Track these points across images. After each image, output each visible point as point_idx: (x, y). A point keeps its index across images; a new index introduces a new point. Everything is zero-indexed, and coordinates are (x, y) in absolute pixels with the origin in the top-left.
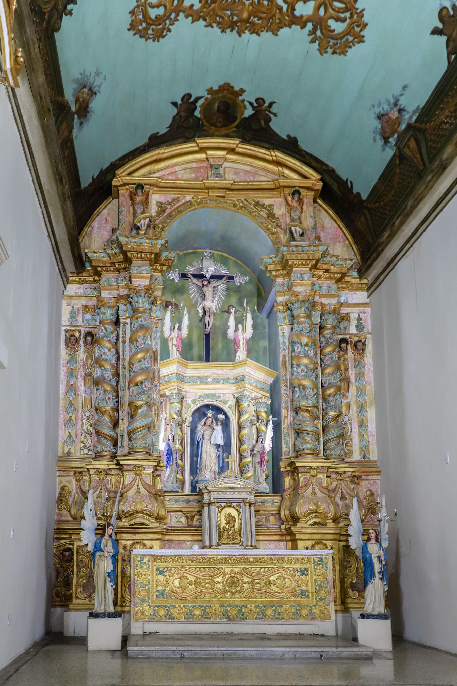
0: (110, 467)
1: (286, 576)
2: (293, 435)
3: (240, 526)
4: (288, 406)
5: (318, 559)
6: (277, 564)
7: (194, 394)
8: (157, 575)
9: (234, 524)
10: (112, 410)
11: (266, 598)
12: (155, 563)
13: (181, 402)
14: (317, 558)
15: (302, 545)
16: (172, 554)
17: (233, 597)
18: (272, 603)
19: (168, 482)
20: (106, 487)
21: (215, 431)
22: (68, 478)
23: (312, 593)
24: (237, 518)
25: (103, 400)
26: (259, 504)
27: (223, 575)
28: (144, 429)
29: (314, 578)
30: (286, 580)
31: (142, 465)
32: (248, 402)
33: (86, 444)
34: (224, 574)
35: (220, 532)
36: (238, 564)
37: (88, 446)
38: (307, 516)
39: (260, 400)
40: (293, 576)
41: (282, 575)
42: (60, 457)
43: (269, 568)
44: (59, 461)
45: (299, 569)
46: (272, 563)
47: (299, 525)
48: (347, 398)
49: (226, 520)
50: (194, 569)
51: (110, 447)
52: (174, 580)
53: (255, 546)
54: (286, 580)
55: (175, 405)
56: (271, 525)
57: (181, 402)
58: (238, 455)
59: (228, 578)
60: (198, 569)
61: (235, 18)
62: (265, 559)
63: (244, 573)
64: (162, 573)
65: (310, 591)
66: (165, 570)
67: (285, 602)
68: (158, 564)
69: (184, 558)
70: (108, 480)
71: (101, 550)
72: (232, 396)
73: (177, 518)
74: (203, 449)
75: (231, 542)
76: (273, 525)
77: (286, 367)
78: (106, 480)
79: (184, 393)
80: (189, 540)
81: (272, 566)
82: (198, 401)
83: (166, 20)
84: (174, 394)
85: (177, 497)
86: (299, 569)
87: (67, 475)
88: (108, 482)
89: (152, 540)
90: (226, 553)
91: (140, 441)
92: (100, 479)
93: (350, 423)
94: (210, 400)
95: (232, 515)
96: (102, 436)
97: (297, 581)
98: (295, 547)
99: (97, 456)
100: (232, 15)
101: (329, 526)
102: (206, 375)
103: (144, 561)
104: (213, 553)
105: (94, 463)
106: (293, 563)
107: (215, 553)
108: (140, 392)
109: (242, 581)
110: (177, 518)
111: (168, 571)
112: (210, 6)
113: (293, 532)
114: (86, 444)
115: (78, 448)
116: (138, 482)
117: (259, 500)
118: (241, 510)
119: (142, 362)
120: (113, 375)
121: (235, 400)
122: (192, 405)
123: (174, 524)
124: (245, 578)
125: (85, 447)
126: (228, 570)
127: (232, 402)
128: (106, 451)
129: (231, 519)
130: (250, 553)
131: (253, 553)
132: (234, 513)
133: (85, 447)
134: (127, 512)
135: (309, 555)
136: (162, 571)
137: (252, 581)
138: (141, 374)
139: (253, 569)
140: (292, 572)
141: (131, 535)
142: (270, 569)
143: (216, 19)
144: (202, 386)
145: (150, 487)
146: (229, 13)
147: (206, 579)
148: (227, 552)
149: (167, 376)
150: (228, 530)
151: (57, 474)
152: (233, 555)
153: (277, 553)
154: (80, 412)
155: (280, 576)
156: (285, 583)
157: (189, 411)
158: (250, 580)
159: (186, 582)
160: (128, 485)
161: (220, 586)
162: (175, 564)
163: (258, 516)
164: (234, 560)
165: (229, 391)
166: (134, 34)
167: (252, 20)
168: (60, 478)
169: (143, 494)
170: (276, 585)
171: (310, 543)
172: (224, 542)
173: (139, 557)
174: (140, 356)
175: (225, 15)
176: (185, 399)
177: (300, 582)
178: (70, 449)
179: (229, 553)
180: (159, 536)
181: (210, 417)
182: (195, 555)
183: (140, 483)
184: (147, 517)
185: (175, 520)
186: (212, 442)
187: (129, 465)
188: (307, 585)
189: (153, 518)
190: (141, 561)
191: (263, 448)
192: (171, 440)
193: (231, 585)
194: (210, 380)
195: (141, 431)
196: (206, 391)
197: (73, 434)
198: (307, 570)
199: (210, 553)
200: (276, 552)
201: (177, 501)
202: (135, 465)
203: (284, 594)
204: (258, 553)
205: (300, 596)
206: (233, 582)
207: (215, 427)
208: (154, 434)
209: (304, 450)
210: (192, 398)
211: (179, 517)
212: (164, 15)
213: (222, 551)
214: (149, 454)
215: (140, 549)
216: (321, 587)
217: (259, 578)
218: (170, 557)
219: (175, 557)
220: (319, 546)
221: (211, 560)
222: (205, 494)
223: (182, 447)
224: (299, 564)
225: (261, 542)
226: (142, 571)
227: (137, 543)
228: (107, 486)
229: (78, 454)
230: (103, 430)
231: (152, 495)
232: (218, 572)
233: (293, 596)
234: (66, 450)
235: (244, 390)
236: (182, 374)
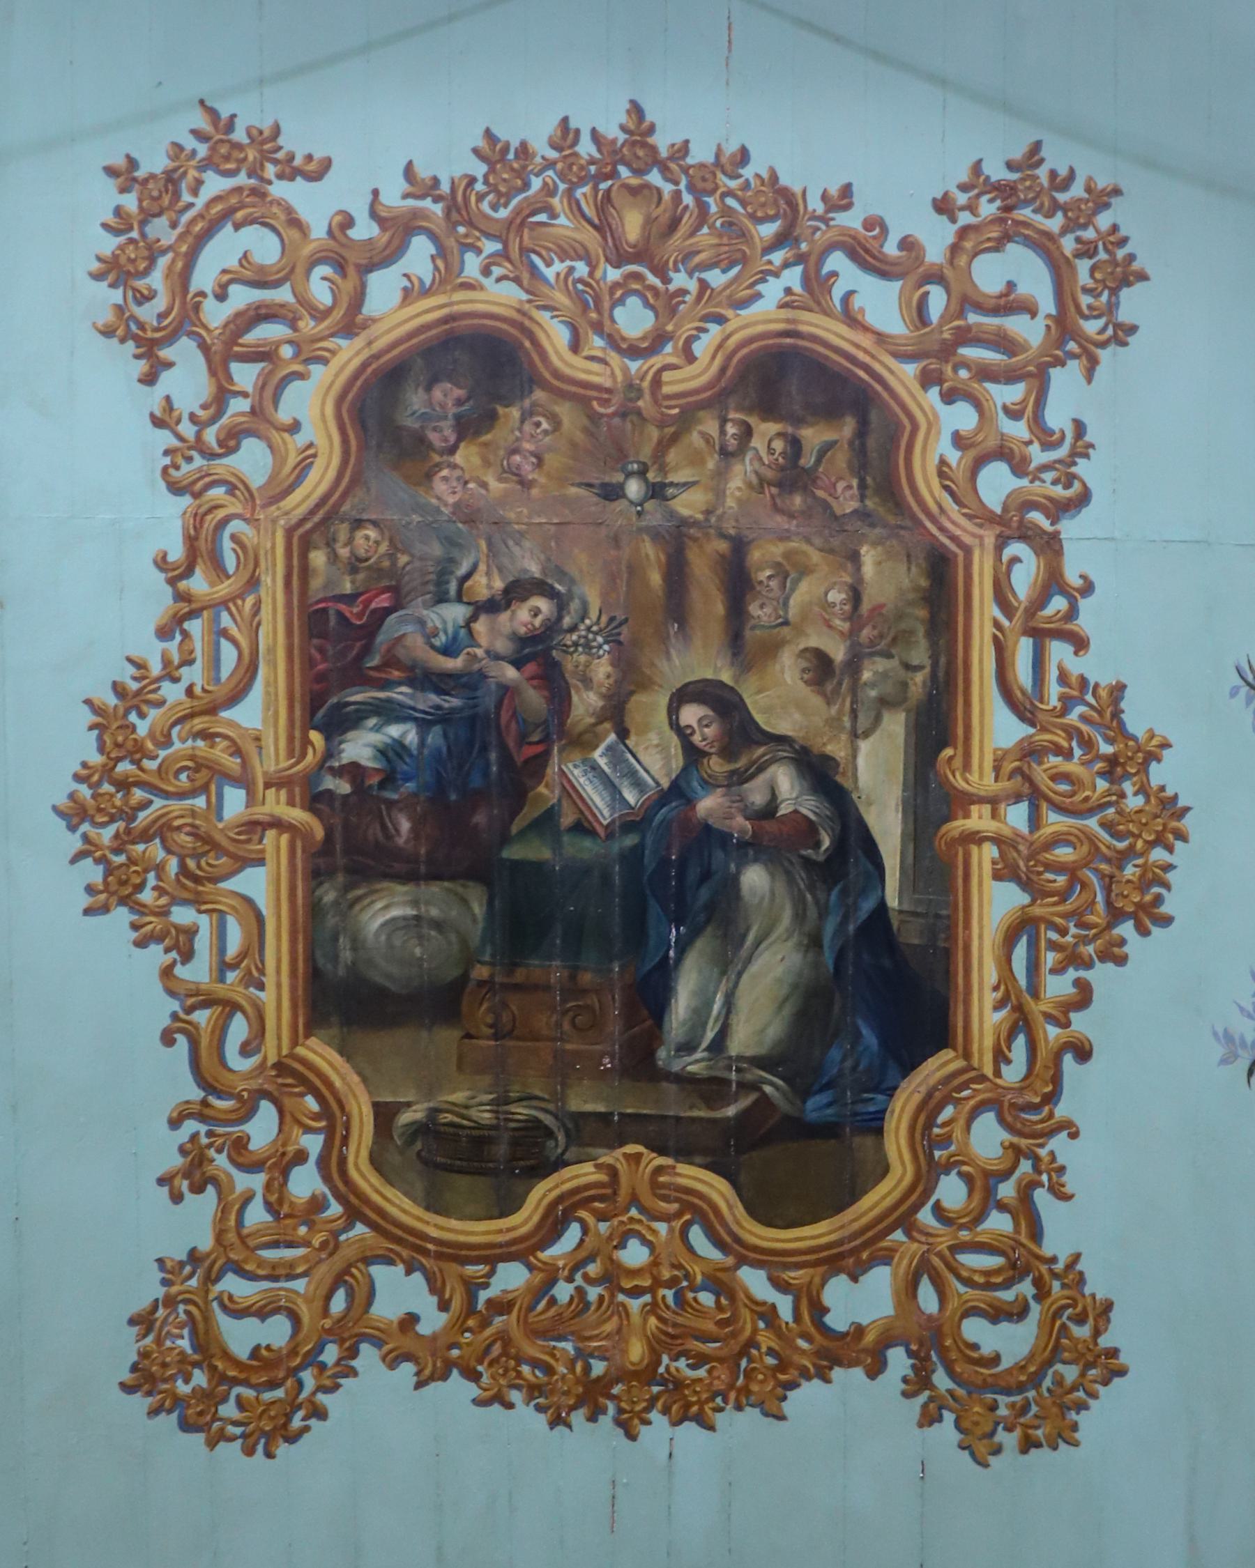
61: (598, 1368)
83: (301, 1367)
100: (583, 1355)
112: (485, 1323)
143: (519, 1375)
146: (568, 1346)
166: (154, 1412)
167: (667, 1368)
175: (553, 1356)
212: (293, 1352)
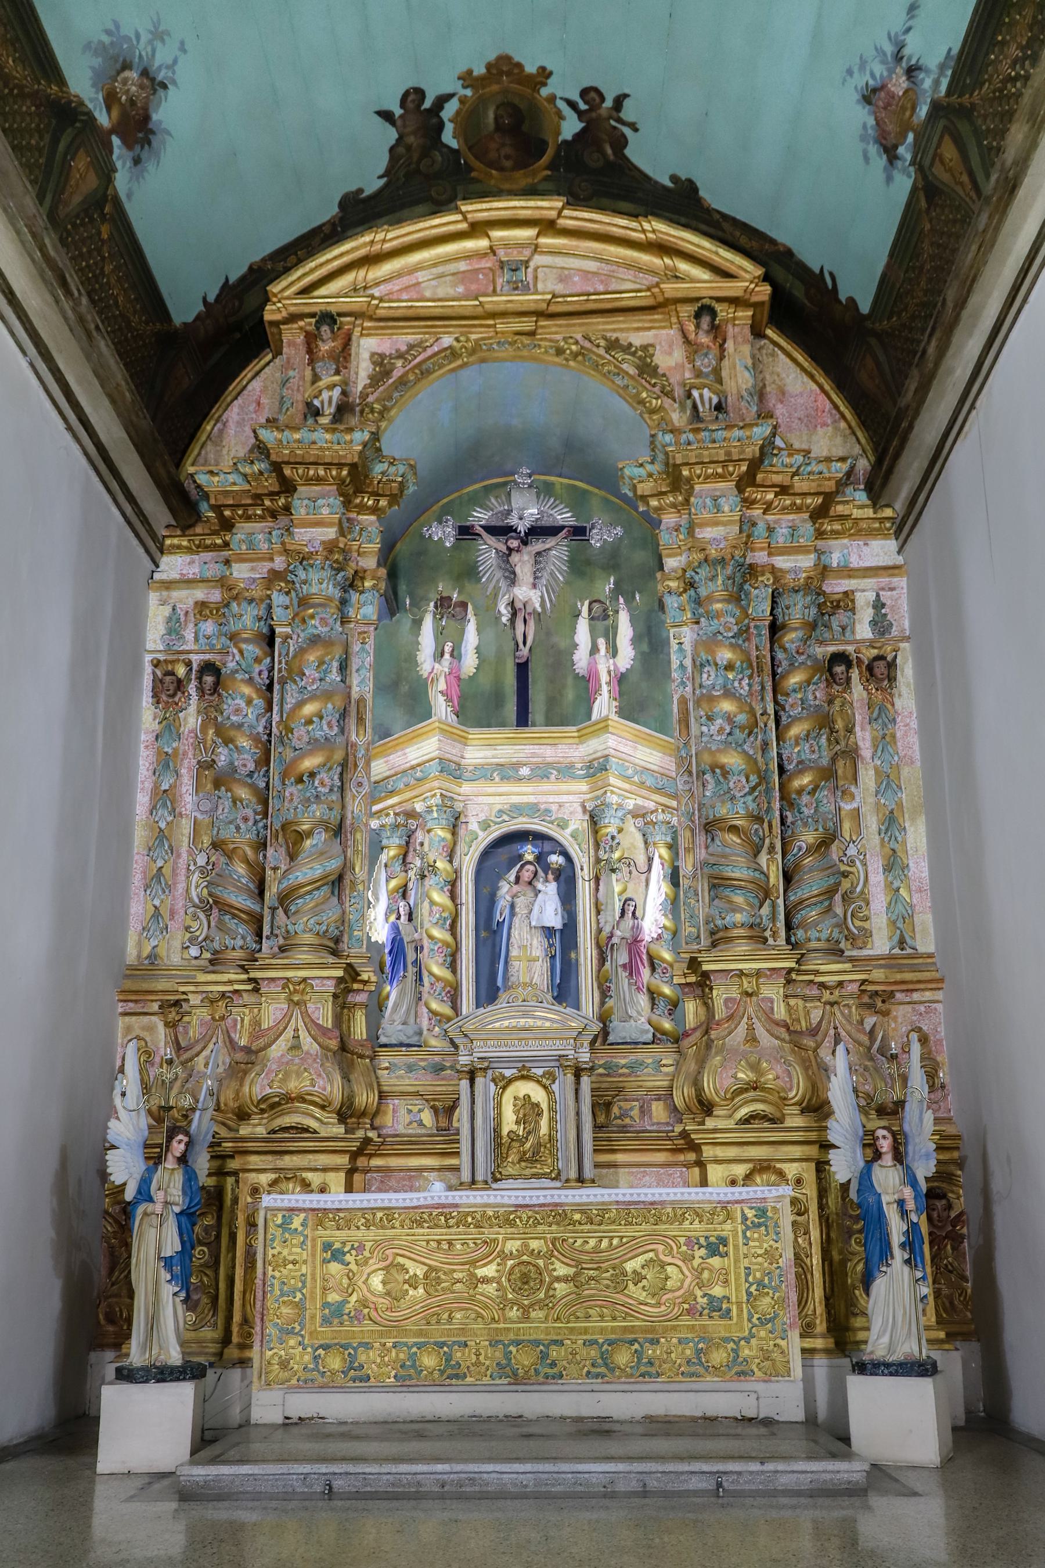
0: (237, 987)
1: (669, 1260)
2: (706, 894)
3: (550, 1128)
4: (693, 822)
5: (753, 1212)
6: (643, 1227)
7: (486, 808)
8: (325, 1261)
9: (537, 1122)
10: (251, 847)
11: (614, 1319)
12: (321, 1232)
13: (454, 830)
14: (751, 1208)
15: (720, 1175)
16: (365, 1205)
17: (526, 1317)
18: (632, 1333)
19: (394, 1021)
20: (229, 1036)
21: (540, 895)
22: (146, 1019)
23: (739, 1304)
24: (544, 1106)
25: (231, 822)
26: (621, 1071)
27: (498, 1260)
28: (318, 889)
29: (746, 1263)
30: (669, 1269)
31: (305, 980)
32: (617, 821)
33: (197, 933)
34: (504, 1256)
35: (499, 1145)
36: (540, 1228)
37: (200, 939)
38: (733, 1099)
39: (653, 817)
40: (688, 1259)
41: (657, 1255)
42: (131, 968)
43: (622, 1237)
44: (127, 977)
45: (702, 1241)
46: (631, 1224)
47: (710, 1123)
49: (516, 1112)
50: (424, 1243)
51: (243, 938)
52: (369, 1275)
53: (593, 1181)
54: (669, 1269)
55: (436, 835)
56: (653, 1125)
57: (454, 830)
58: (595, 952)
59: (513, 1268)
60: (433, 1244)
62: (613, 1214)
63: (556, 1253)
64: (337, 1256)
65: (734, 1300)
66: (346, 1250)
67: (666, 1330)
68: (328, 1232)
69: (396, 1216)
70: (236, 1020)
71: (151, 1200)
72: (580, 809)
73: (410, 1111)
74: (512, 940)
75: (528, 1172)
76: (658, 1124)
77: (688, 727)
78: (229, 1021)
79: (459, 806)
80: (433, 1169)
81: (630, 1232)
82: (496, 823)
84: (435, 809)
85: (411, 1060)
86: (702, 1241)
87: (145, 1010)
88: (235, 1025)
89: (325, 1170)
90: (506, 1201)
91: (305, 919)
92: (213, 1019)
94: (524, 820)
95: (533, 1100)
96: (227, 912)
97: (699, 1272)
98: (704, 1182)
99: (216, 962)
101: (789, 1123)
102: (515, 760)
103: (293, 1226)
104: (472, 1200)
105: (202, 977)
106: (687, 1222)
107: (479, 1200)
108: (309, 799)
109: (550, 1276)
110: (410, 1111)
111: (354, 1252)
113: (693, 1140)
114: (197, 933)
115: (177, 944)
116: (297, 1021)
117: (623, 1062)
118: (555, 1087)
119: (314, 726)
120: (257, 763)
121: (587, 817)
122: (481, 834)
123: (401, 1129)
124: (558, 1265)
125: (193, 940)
126: (513, 1246)
127: (578, 822)
128: (234, 949)
129: (528, 1110)
130: (570, 1200)
131: (577, 1200)
132: (538, 1095)
133: (193, 940)
134: (264, 1099)
135: (728, 1202)
136: (338, 1250)
137: (576, 1274)
138: (311, 753)
139: (579, 1242)
140: (684, 1248)
141: (269, 1158)
142: (624, 1240)
144: (506, 788)
145: (324, 1034)
147: (454, 1271)
148: (510, 1197)
149: (419, 765)
150: (522, 1141)
151: (120, 1010)
152: (527, 1206)
153: (642, 1198)
154: (184, 855)
155: (651, 1260)
156: (667, 1278)
157: (472, 849)
158: (571, 1271)
159: (400, 1278)
160: (269, 1029)
161: (491, 1289)
162: (373, 1233)
163: (622, 1104)
164: (529, 1218)
165: (571, 798)
168: (127, 1019)
169: (307, 1053)
170: (640, 1285)
171: (740, 1170)
172: (510, 1170)
173: (280, 1216)
174: (309, 709)
176: (463, 819)
177: (706, 1275)
178: (156, 946)
179: (513, 1201)
180: (344, 1160)
181: (529, 863)
182: (427, 1207)
183: (301, 1023)
184: (317, 1112)
185: (404, 1117)
186: (533, 924)
187: (273, 979)
188: (726, 1281)
189: (329, 1112)
190: (284, 1226)
191: (637, 929)
192: (402, 918)
193: (519, 1284)
194: (525, 771)
195: (310, 892)
196: (515, 799)
197: (165, 912)
198: (724, 1241)
199: (464, 1200)
200: (639, 1195)
201: (410, 1068)
202: (287, 979)
203: (663, 1308)
204: (592, 1199)
205: (706, 1312)
206: (525, 1279)
207: (540, 886)
208: (353, 901)
210: (482, 817)
211: (415, 1109)
213: (495, 1196)
214: (335, 953)
215: (293, 1193)
216: (764, 1287)
217: (595, 1266)
218: (360, 1214)
219: (374, 1215)
220: (765, 1177)
221: (470, 1220)
222: (462, 1047)
223: (455, 938)
224: (703, 1226)
225: (622, 1170)
226: (285, 1252)
227: (288, 1179)
228: (233, 1035)
229: (176, 959)
230: (226, 895)
231: (329, 1054)
232: (485, 1250)
233: (689, 1312)
234: (147, 951)
235: (606, 792)
236: (455, 759)
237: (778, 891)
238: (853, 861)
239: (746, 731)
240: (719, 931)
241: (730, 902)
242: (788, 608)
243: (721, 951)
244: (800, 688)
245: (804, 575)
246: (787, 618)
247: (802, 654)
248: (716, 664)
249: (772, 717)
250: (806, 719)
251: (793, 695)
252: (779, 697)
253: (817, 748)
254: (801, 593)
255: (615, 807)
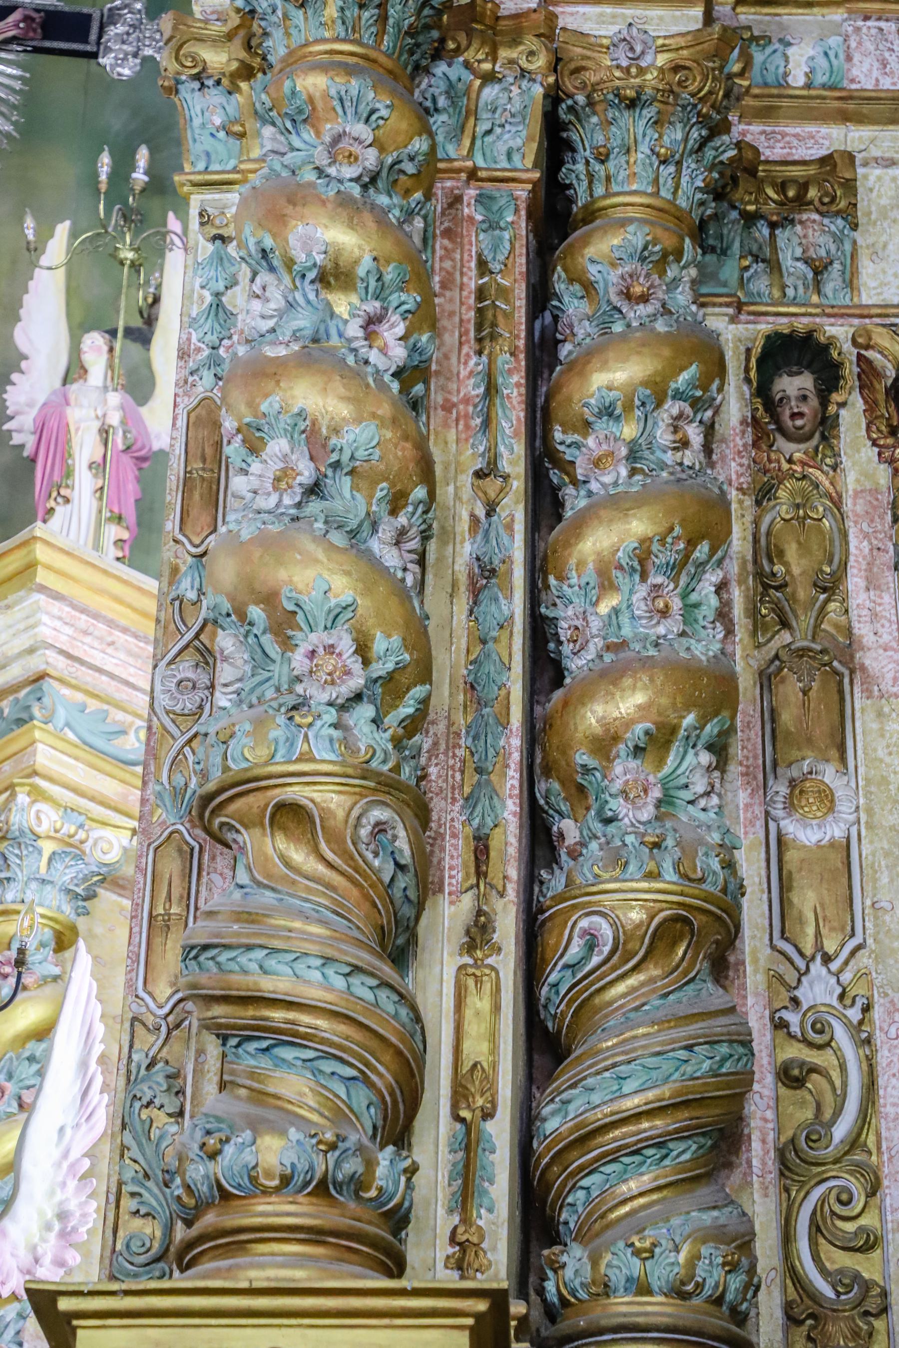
48: (827, 799)
93: (856, 1029)
209: (225, 1196)
237: (490, 1087)
238: (820, 1028)
239: (382, 490)
240: (201, 1207)
241: (260, 1097)
242: (603, 159)
243: (204, 1277)
244: (629, 407)
245: (662, 60)
246: (599, 190)
247: (644, 299)
248: (289, 263)
249: (518, 485)
250: (639, 501)
251: (602, 426)
252: (558, 435)
253: (676, 604)
254: (649, 113)
255: (48, 847)
